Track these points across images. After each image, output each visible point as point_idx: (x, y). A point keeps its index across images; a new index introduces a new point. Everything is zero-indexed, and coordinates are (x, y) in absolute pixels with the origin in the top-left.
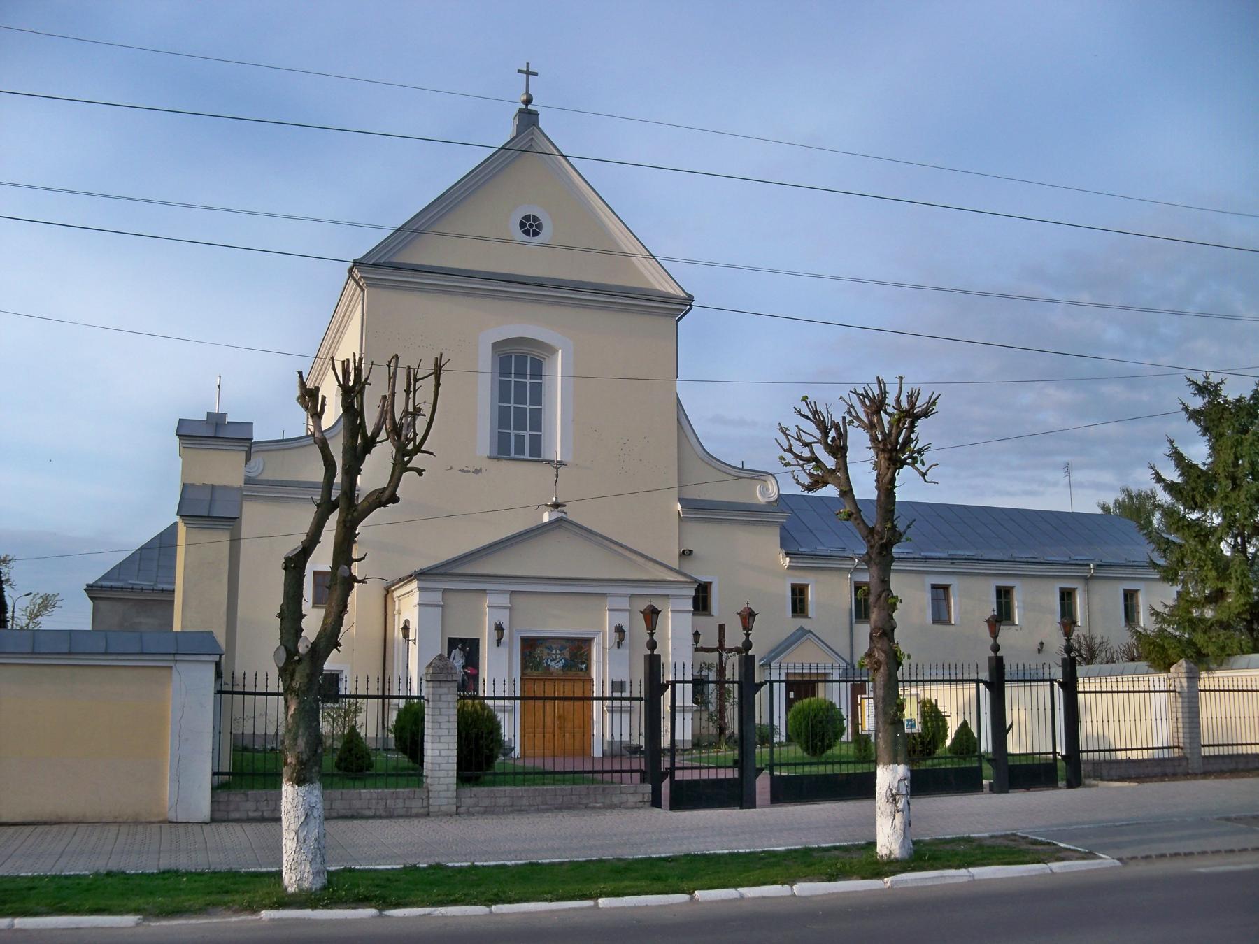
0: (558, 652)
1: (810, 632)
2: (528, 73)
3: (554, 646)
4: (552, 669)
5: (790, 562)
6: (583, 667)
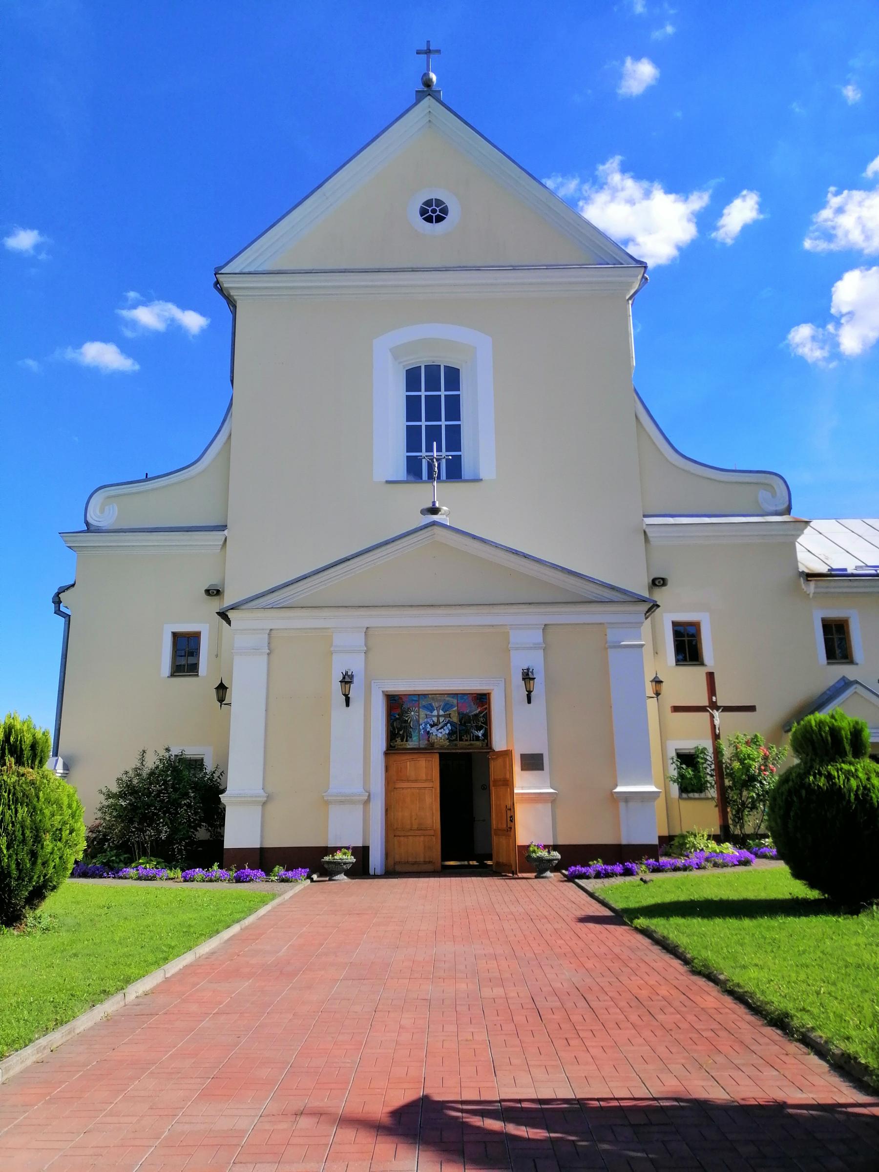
0: (441, 713)
1: (857, 682)
3: (436, 705)
5: (816, 588)
6: (480, 735)
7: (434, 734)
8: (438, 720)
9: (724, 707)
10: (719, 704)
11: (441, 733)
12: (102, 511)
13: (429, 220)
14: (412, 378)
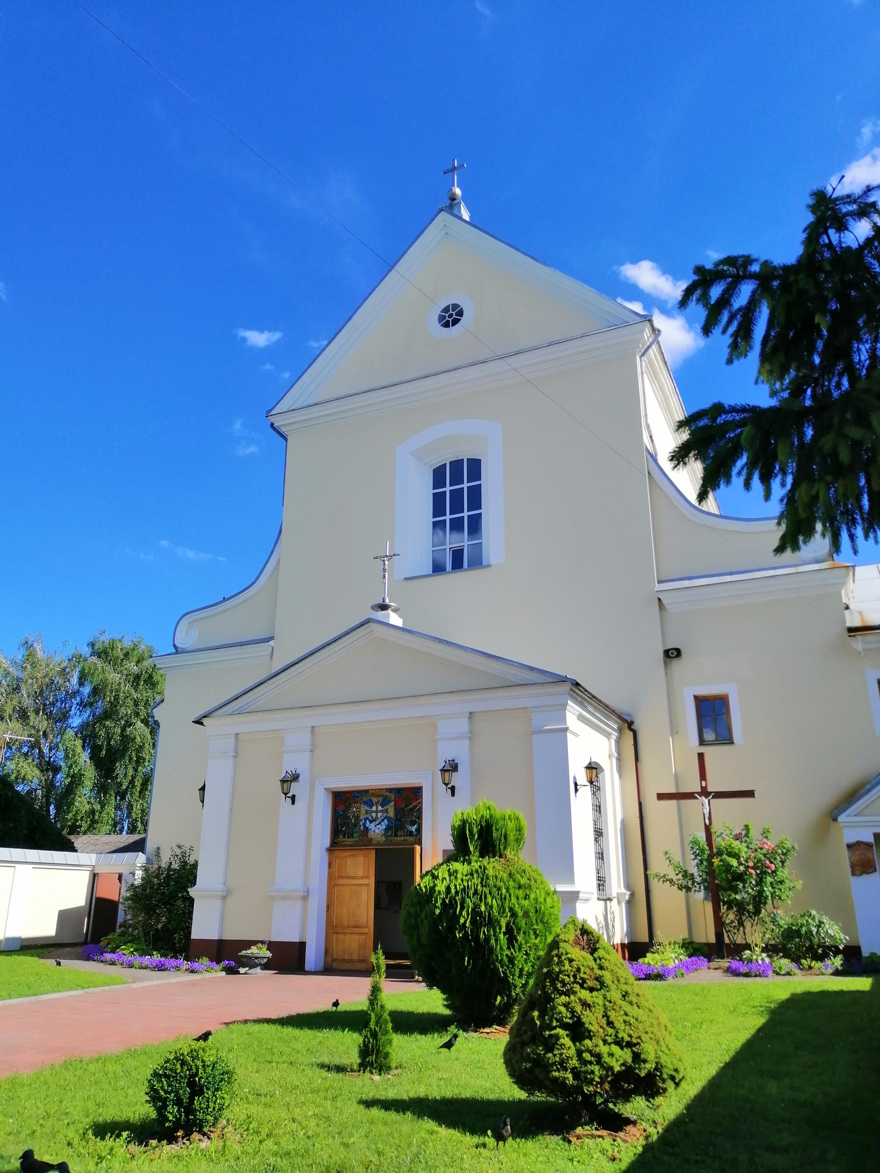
0: (380, 808)
3: (375, 800)
4: (371, 834)
7: (372, 830)
8: (377, 816)
9: (715, 792)
10: (709, 790)
11: (379, 828)
12: (187, 634)
13: (446, 325)
14: (438, 476)
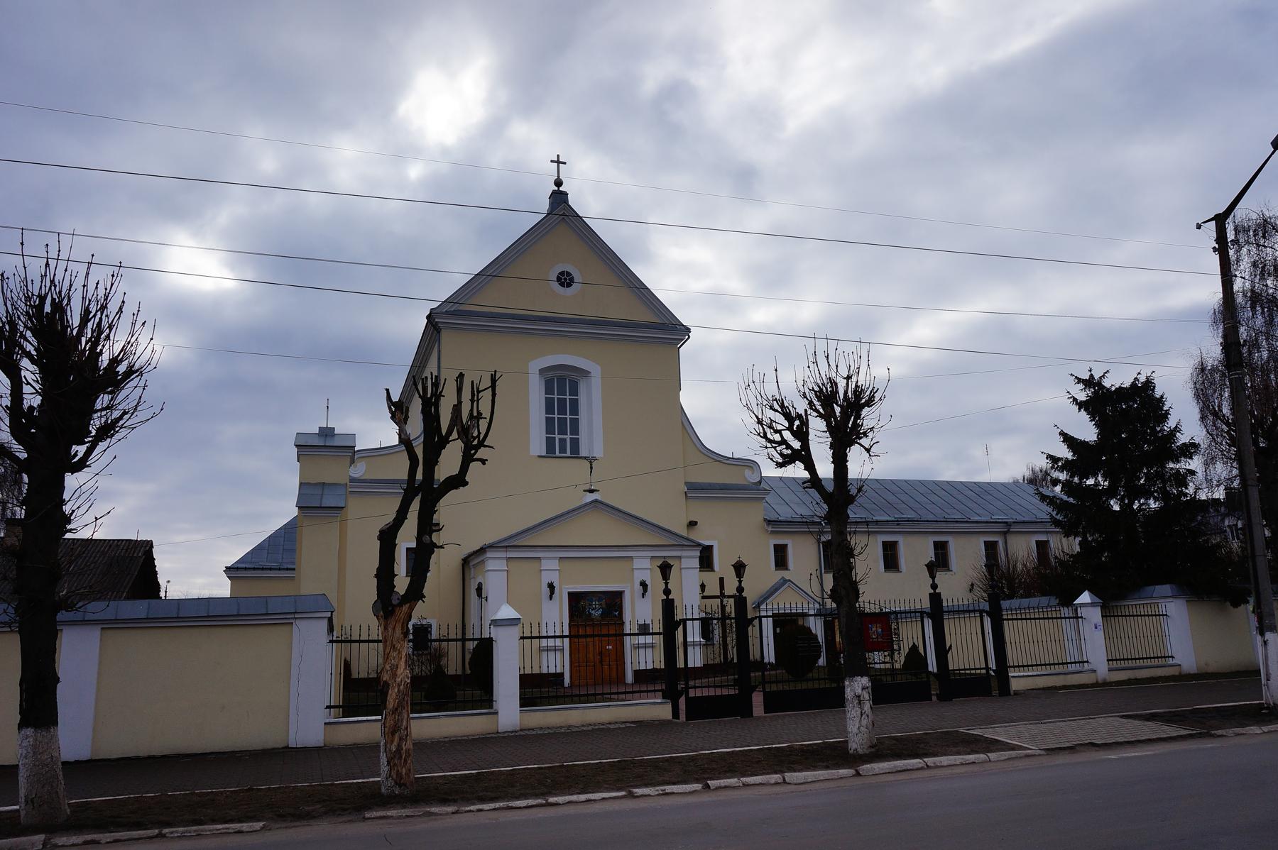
0: (597, 603)
1: (790, 581)
2: (558, 162)
13: (562, 285)
